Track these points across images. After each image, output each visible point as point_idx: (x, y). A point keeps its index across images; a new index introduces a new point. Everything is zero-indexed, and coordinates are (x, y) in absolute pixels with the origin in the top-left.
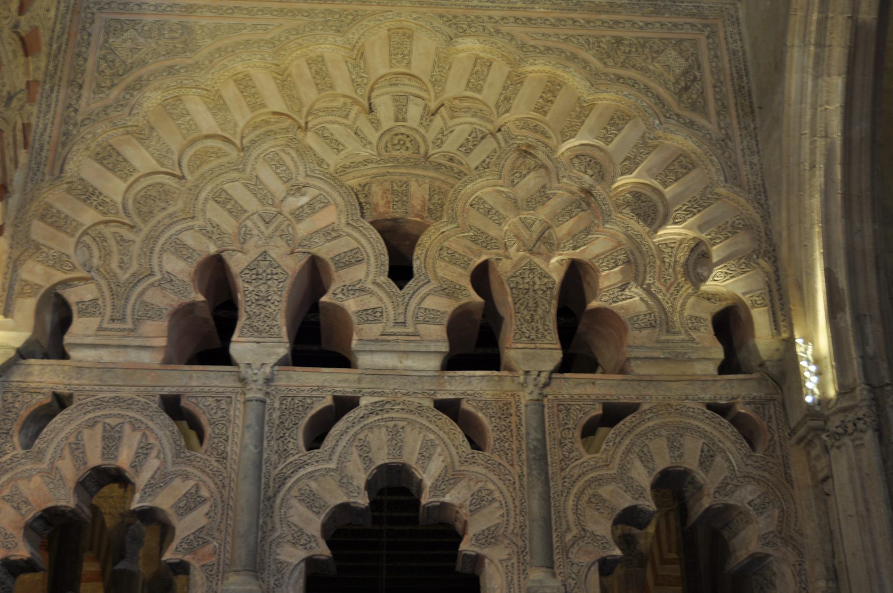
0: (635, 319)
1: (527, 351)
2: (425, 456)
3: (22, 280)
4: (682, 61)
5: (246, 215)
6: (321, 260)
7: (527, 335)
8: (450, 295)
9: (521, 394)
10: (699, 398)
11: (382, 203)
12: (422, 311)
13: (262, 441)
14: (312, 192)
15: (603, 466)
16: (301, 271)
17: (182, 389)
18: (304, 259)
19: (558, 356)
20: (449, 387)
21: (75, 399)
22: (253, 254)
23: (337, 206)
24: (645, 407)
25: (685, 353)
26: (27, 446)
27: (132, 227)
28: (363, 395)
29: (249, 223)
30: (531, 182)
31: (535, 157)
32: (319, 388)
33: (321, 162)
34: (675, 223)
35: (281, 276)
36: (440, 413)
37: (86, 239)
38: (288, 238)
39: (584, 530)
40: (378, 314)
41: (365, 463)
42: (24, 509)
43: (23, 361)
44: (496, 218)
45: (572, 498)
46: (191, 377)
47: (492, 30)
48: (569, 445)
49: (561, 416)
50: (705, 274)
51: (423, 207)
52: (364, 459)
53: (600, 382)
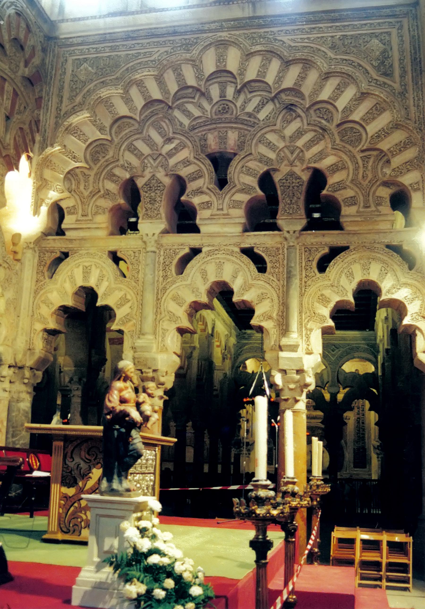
0: (346, 200)
2: (235, 277)
3: (41, 199)
4: (381, 45)
8: (246, 193)
14: (176, 142)
16: (172, 184)
17: (118, 248)
18: (173, 178)
19: (304, 222)
21: (70, 254)
23: (189, 148)
24: (351, 247)
31: (295, 111)
33: (181, 124)
35: (162, 187)
36: (243, 255)
40: (209, 205)
42: (50, 307)
44: (273, 147)
46: (121, 242)
51: (235, 144)
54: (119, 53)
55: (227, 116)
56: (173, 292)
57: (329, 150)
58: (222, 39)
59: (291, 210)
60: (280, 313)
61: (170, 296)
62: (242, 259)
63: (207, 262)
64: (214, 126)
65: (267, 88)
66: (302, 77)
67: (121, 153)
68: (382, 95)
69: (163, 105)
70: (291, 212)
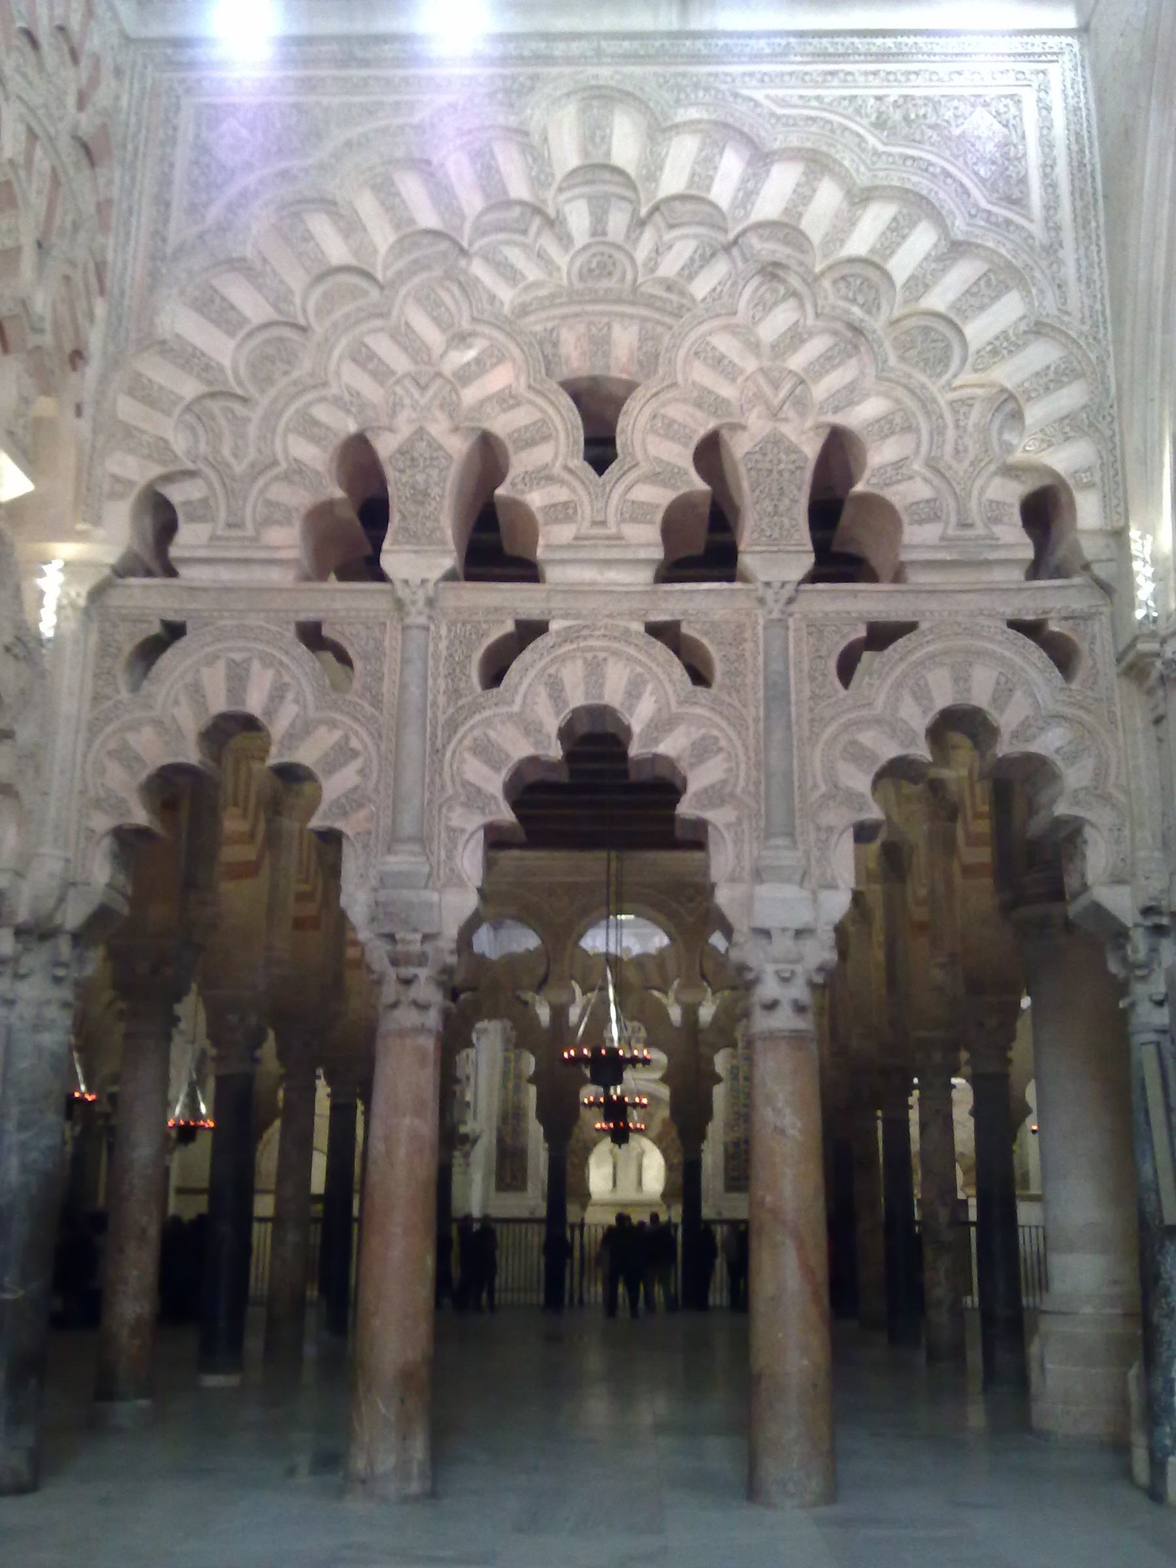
1: (767, 555)
2: (634, 692)
4: (998, 127)
5: (394, 379)
6: (496, 438)
7: (768, 533)
8: (665, 484)
10: (998, 613)
11: (575, 355)
13: (425, 679)
15: (864, 706)
19: (808, 561)
20: (664, 605)
22: (405, 429)
23: (514, 360)
24: (924, 626)
26: (135, 688)
27: (244, 400)
28: (553, 618)
29: (399, 390)
30: (781, 318)
31: (783, 281)
32: (496, 609)
36: (653, 639)
37: (189, 418)
38: (451, 407)
39: (836, 787)
40: (571, 511)
43: (120, 581)
45: (820, 745)
48: (820, 678)
50: (1015, 442)
54: (325, 101)
55: (605, 284)
56: (476, 733)
57: (869, 382)
58: (602, 82)
59: (777, 529)
60: (752, 788)
61: (467, 742)
62: (652, 651)
63: (563, 659)
64: (576, 308)
65: (714, 218)
66: (803, 197)
67: (332, 367)
68: (1003, 251)
69: (444, 245)
70: (776, 535)
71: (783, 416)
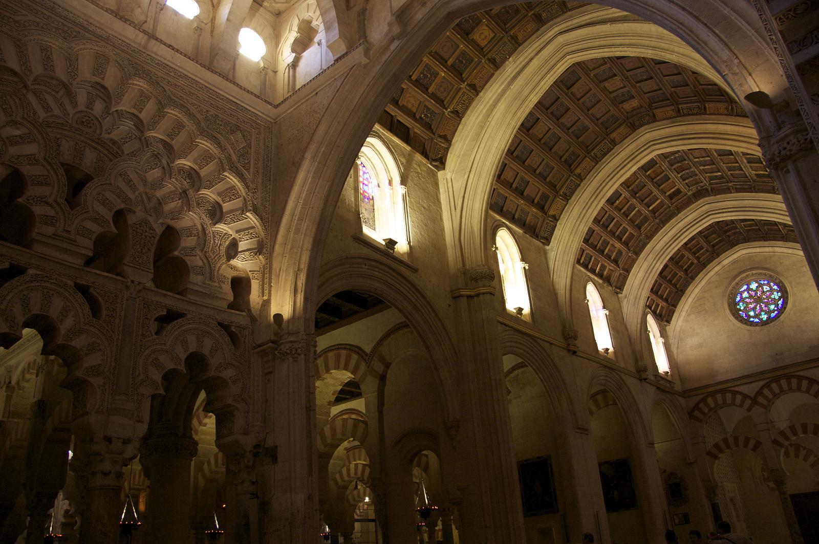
9: (125, 292)
12: (82, 228)
15: (162, 344)
24: (189, 316)
25: (216, 293)
28: (31, 268)
34: (225, 224)
36: (78, 292)
39: (147, 377)
41: (25, 311)
47: (154, 81)
48: (147, 328)
49: (145, 311)
50: (233, 255)
52: (24, 308)
53: (168, 297)
71: (150, 213)
